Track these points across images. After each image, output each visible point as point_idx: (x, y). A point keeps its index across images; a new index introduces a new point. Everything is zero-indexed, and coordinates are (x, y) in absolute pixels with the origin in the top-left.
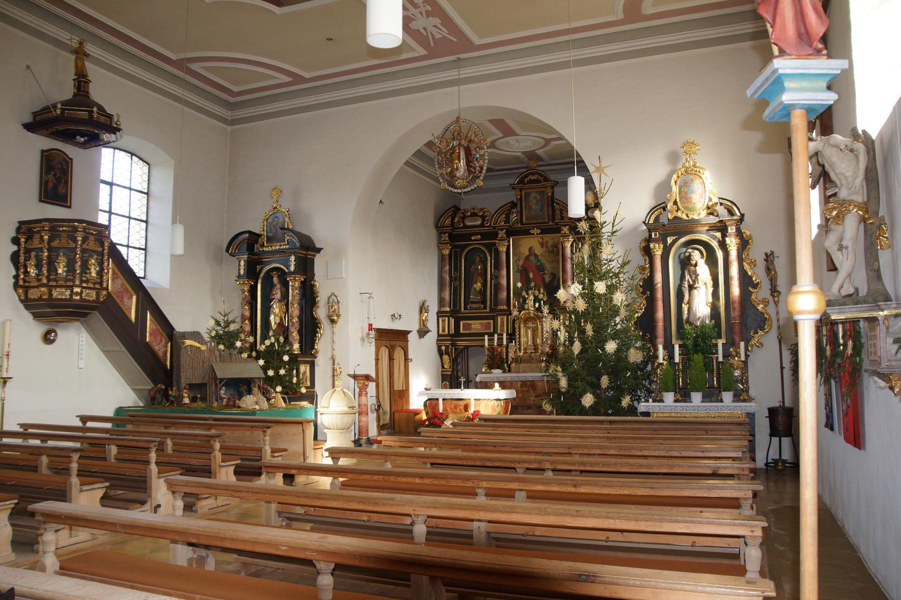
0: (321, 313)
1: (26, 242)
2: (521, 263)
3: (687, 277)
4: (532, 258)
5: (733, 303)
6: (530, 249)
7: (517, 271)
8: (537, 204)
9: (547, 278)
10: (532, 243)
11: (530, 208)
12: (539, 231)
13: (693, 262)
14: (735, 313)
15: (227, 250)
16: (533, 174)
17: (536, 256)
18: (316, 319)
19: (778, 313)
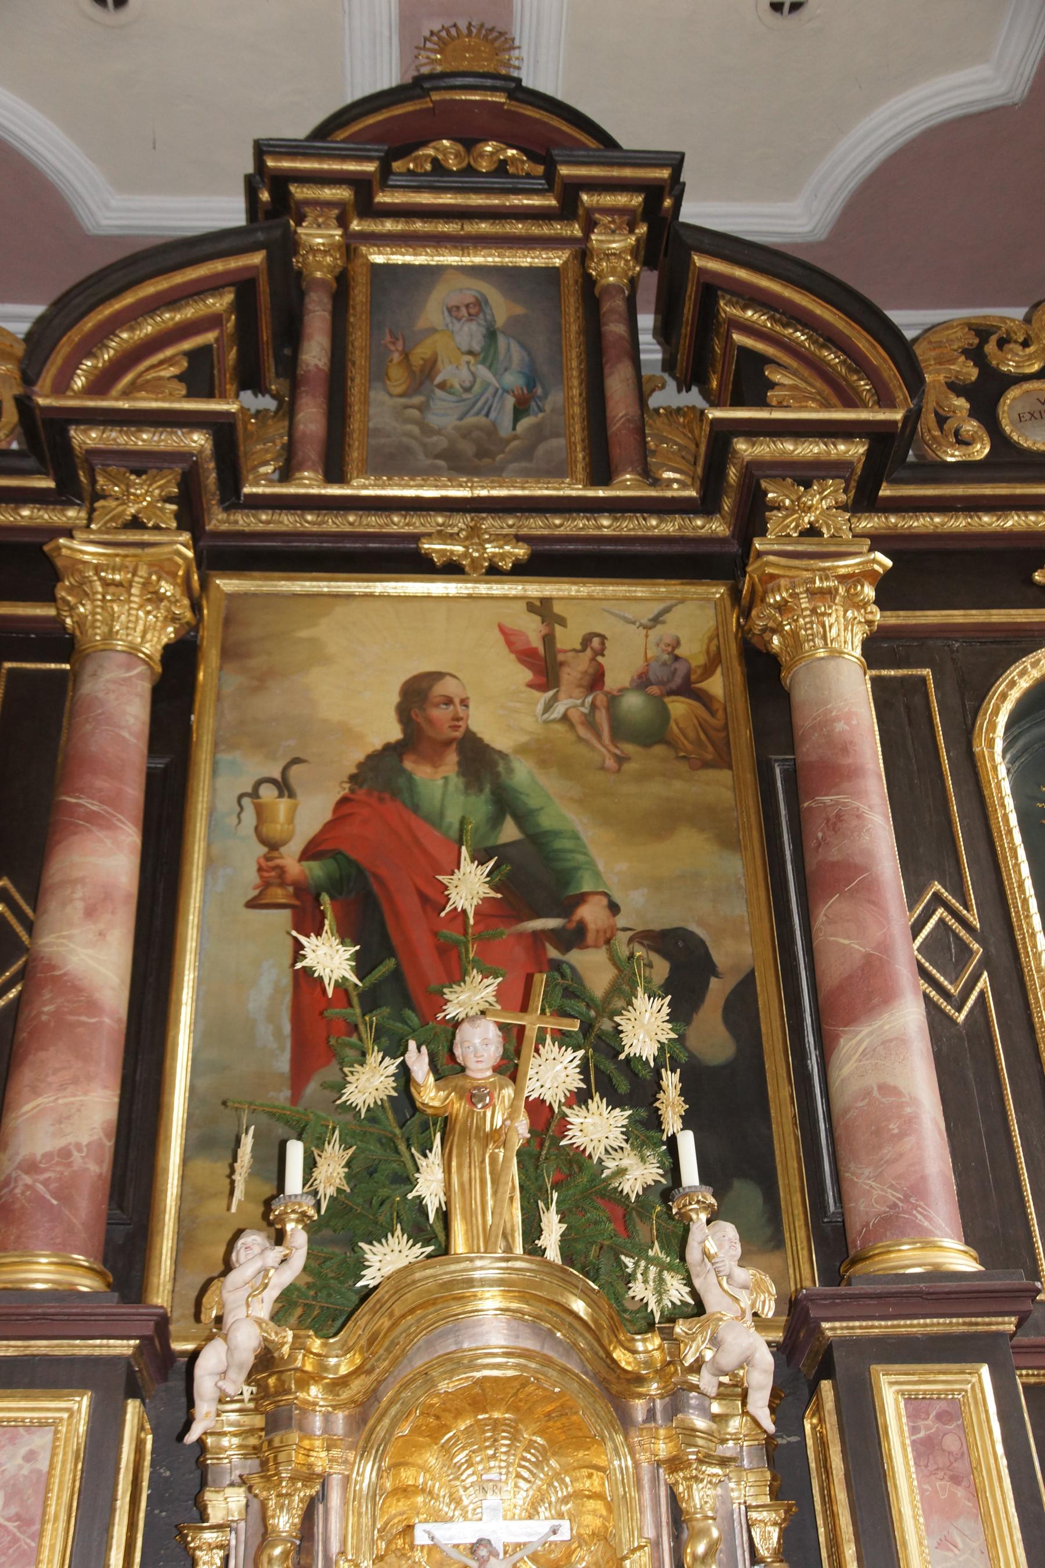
2: (310, 813)
4: (437, 782)
6: (416, 694)
8: (487, 352)
11: (424, 377)
17: (477, 760)
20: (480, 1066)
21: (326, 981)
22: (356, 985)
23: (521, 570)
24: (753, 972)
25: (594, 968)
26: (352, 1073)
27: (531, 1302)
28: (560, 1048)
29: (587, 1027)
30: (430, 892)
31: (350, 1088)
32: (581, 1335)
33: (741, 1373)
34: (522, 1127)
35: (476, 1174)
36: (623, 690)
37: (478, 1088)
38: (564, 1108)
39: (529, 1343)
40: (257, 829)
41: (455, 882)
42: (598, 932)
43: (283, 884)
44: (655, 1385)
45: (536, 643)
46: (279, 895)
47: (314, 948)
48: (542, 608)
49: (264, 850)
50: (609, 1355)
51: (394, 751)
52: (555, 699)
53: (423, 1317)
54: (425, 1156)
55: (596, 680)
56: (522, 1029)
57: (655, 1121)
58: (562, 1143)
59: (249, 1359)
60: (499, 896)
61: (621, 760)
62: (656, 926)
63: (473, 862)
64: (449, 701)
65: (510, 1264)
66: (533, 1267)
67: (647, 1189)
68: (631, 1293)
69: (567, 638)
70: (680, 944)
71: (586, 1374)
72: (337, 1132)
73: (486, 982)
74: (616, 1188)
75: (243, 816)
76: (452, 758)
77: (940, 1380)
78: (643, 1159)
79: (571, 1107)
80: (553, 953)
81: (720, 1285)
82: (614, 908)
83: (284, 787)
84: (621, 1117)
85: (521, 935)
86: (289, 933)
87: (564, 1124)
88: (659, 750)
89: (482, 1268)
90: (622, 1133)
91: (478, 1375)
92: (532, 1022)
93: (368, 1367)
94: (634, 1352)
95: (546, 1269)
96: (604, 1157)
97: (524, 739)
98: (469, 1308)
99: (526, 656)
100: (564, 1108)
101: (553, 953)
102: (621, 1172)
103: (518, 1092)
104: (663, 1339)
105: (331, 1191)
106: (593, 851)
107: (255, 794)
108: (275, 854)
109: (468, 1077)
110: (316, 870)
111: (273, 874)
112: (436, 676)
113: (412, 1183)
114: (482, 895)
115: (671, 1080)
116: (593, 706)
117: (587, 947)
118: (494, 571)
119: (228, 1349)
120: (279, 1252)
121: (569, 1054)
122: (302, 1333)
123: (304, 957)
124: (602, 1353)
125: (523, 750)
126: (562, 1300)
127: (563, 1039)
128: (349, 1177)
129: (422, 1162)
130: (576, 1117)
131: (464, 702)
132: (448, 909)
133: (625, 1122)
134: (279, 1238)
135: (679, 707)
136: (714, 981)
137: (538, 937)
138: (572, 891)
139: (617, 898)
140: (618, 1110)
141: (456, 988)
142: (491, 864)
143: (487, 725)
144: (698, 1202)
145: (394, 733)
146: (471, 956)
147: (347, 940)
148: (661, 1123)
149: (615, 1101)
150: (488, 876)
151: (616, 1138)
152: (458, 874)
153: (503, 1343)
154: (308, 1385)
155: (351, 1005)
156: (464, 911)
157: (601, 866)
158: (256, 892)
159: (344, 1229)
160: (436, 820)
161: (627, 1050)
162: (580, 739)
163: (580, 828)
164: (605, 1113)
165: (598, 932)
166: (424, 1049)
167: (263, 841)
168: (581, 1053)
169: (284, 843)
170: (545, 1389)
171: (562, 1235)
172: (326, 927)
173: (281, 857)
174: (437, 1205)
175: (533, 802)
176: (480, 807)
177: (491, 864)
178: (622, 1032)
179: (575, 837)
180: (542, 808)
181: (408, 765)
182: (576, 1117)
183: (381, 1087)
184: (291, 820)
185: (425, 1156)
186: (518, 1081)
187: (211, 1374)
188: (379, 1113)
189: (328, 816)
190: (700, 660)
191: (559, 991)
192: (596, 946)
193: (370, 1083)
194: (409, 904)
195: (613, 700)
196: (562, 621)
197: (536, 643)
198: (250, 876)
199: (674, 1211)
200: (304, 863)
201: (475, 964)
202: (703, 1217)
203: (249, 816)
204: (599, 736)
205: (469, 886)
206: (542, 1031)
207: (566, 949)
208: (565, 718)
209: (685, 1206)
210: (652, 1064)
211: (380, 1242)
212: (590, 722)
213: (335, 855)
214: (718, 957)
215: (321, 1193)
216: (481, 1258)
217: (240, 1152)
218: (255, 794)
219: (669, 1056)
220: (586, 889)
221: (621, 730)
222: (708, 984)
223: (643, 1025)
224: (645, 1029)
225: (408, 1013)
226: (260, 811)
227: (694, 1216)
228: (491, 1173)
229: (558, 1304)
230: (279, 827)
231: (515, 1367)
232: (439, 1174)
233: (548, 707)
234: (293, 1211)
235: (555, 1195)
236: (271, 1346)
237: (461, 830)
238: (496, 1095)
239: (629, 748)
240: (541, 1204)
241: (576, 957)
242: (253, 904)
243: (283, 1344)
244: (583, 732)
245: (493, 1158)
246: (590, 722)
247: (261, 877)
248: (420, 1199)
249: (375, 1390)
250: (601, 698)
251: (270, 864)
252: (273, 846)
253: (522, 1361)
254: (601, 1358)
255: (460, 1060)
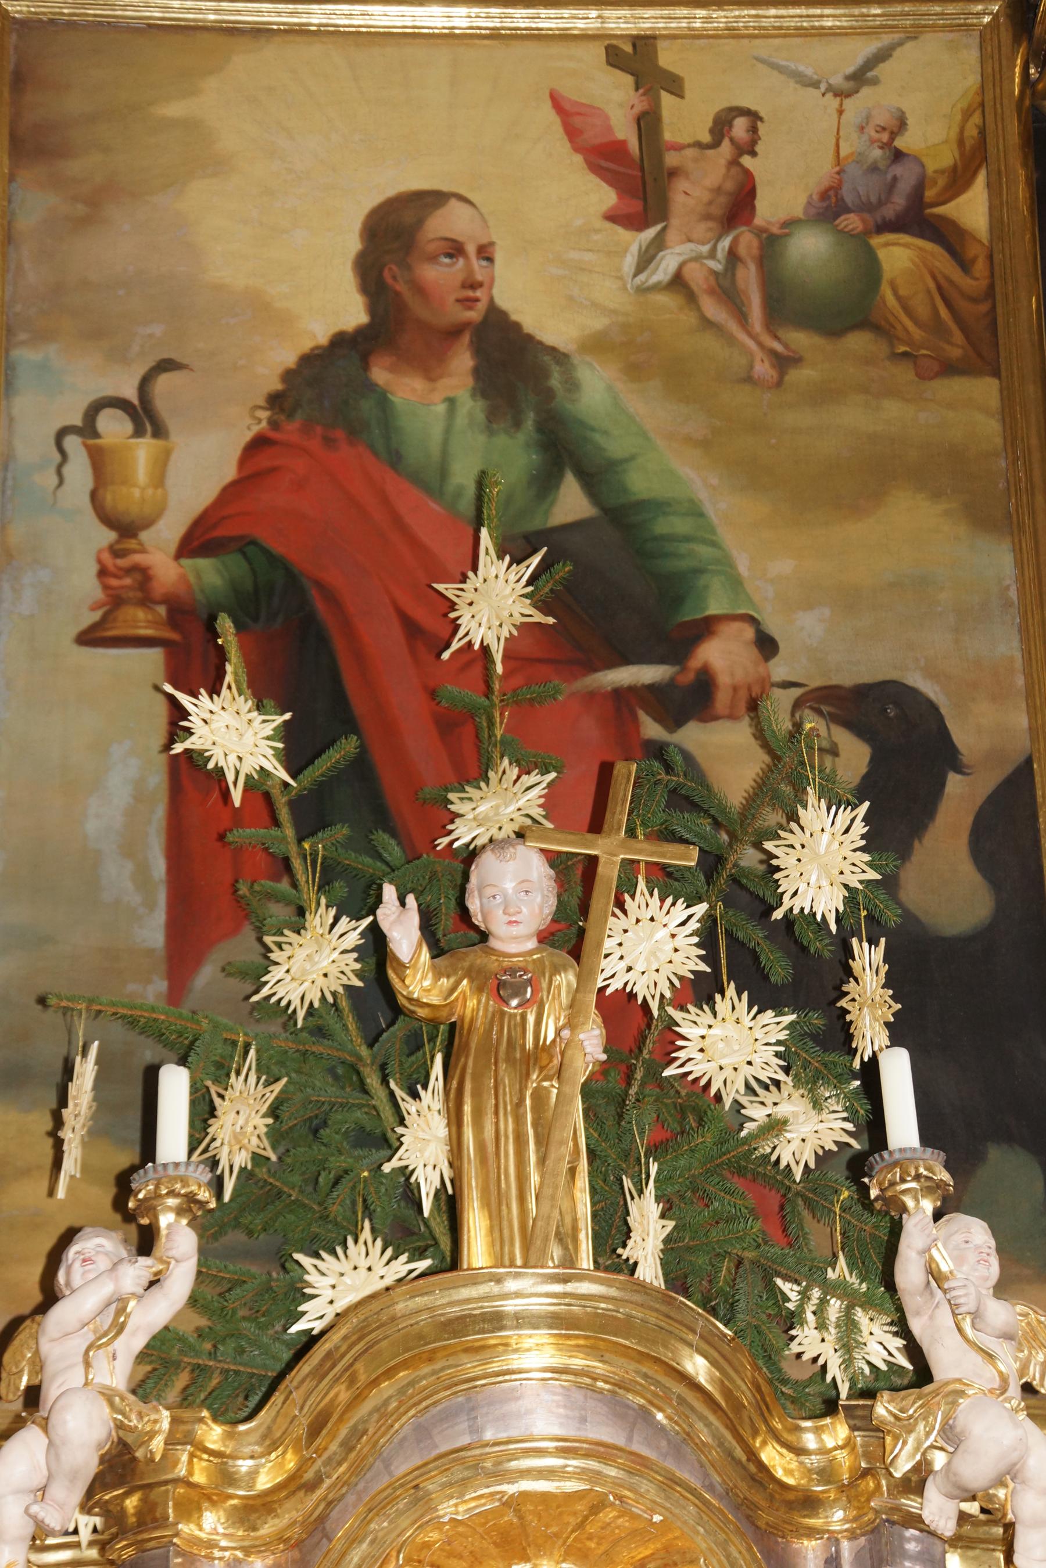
2: (195, 467)
4: (434, 407)
6: (393, 236)
17: (510, 364)
20: (515, 930)
21: (230, 777)
22: (286, 785)
24: (1029, 762)
25: (726, 754)
26: (279, 946)
27: (607, 1356)
28: (662, 901)
29: (712, 862)
30: (420, 614)
31: (276, 973)
32: (702, 1418)
33: (1001, 1493)
34: (591, 1043)
35: (509, 1126)
36: (790, 224)
37: (512, 971)
38: (670, 1010)
39: (605, 1431)
40: (94, 495)
41: (469, 596)
42: (735, 689)
43: (146, 600)
44: (839, 1514)
45: (624, 131)
46: (140, 620)
47: (207, 716)
48: (635, 57)
49: (110, 536)
50: (753, 1456)
51: (351, 348)
52: (659, 244)
53: (411, 1384)
54: (415, 1096)
55: (738, 204)
56: (593, 860)
57: (840, 1034)
58: (666, 1073)
59: (90, 1466)
60: (551, 620)
61: (784, 362)
62: (847, 679)
63: (500, 557)
64: (455, 249)
65: (570, 1287)
66: (613, 1292)
67: (824, 1158)
68: (795, 1348)
69: (685, 120)
70: (891, 712)
71: (711, 1488)
72: (252, 1053)
73: (527, 780)
74: (766, 1157)
75: (66, 470)
76: (463, 361)
78: (817, 1105)
79: (683, 1008)
80: (652, 729)
81: (960, 1330)
82: (766, 645)
83: (144, 416)
84: (776, 1025)
85: (592, 697)
86: (158, 689)
87: (671, 1039)
88: (858, 341)
89: (518, 1295)
90: (777, 1055)
91: (511, 1489)
92: (610, 851)
93: (309, 1475)
94: (800, 1451)
95: (637, 1298)
96: (744, 1100)
97: (597, 323)
98: (495, 1367)
99: (604, 158)
100: (670, 1010)
101: (652, 729)
102: (776, 1126)
103: (584, 979)
104: (853, 1428)
105: (242, 1159)
106: (727, 537)
107: (88, 429)
108: (132, 544)
109: (493, 951)
110: (208, 574)
111: (128, 581)
112: (431, 200)
113: (390, 1145)
114: (519, 620)
115: (869, 960)
116: (733, 256)
117: (716, 718)
119: (51, 1444)
120: (144, 1266)
121: (680, 911)
122: (186, 1414)
123: (189, 732)
124: (739, 1453)
125: (597, 345)
126: (666, 1356)
127: (668, 882)
128: (275, 1136)
129: (409, 1106)
130: (692, 1025)
131: (485, 253)
132: (455, 645)
133: (783, 1036)
134: (146, 1242)
135: (899, 256)
136: (954, 782)
137: (624, 698)
138: (689, 614)
139: (773, 627)
140: (770, 1013)
141: (471, 791)
142: (535, 560)
143: (530, 296)
144: (918, 1177)
145: (352, 312)
146: (499, 732)
147: (268, 703)
148: (850, 1037)
149: (765, 997)
150: (529, 583)
151: (766, 1064)
152: (474, 581)
153: (557, 1431)
154: (200, 1510)
155: (276, 823)
156: (485, 649)
157: (743, 567)
158: (97, 616)
159: (264, 1229)
160: (432, 481)
161: (787, 902)
162: (707, 324)
163: (703, 495)
164: (746, 1021)
165: (735, 689)
166: (411, 900)
167: (108, 520)
168: (701, 909)
169: (148, 523)
170: (634, 1517)
171: (667, 1241)
172: (229, 678)
173: (143, 551)
174: (437, 1183)
175: (616, 447)
176: (514, 456)
177: (535, 560)
178: (778, 869)
179: (696, 512)
180: (632, 458)
181: (379, 375)
182: (692, 1025)
183: (333, 971)
184: (159, 478)
185: (415, 1096)
186: (584, 958)
187: (18, 1492)
188: (331, 1021)
189: (230, 473)
190: (946, 158)
191: (661, 796)
192: (732, 717)
193: (313, 964)
194: (383, 638)
195: (771, 244)
196: (675, 85)
197: (624, 131)
198: (83, 586)
199: (874, 1193)
200: (186, 562)
201: (507, 748)
202: (928, 1206)
203: (79, 472)
204: (742, 317)
205: (494, 603)
206: (630, 865)
207: (675, 720)
208: (678, 282)
209: (892, 1184)
210: (833, 928)
211: (333, 1253)
212: (726, 290)
213: (244, 545)
214: (963, 736)
215: (224, 1163)
216: (517, 1275)
217: (73, 1089)
218: (88, 429)
219: (863, 913)
220: (714, 608)
221: (784, 304)
222: (943, 785)
223: (817, 855)
224: (821, 863)
225: (382, 837)
226: (98, 459)
227: (910, 1203)
228: (535, 1125)
229: (657, 1360)
230: (136, 493)
231: (582, 1474)
232: (439, 1127)
233: (646, 261)
234: (172, 1193)
235: (654, 1168)
236: (129, 1439)
237: (480, 499)
238: (544, 985)
239: (800, 339)
240: (627, 1183)
241: (693, 737)
242: (89, 638)
243: (152, 1435)
244: (712, 309)
245: (540, 1097)
246: (726, 290)
247: (106, 587)
248: (406, 1172)
249: (322, 1519)
250: (747, 241)
251: (121, 562)
252: (126, 528)
253: (593, 1464)
254: (739, 1462)
255: (478, 920)
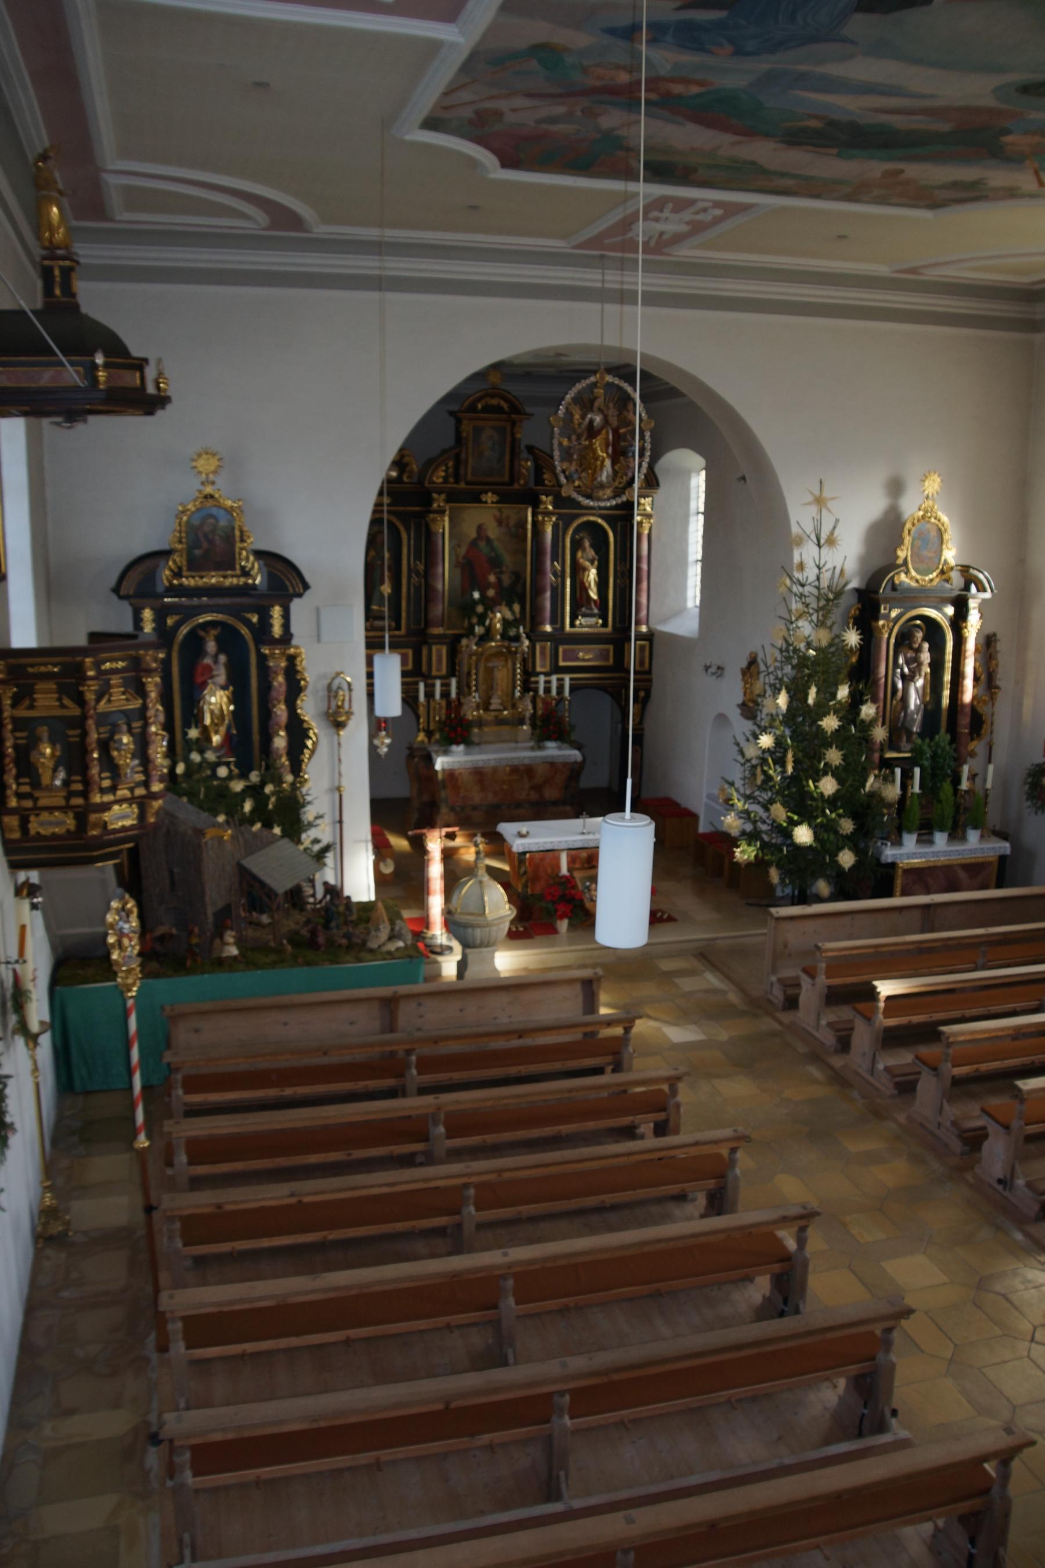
0: (309, 708)
1: (13, 706)
2: (463, 551)
3: (901, 661)
4: (482, 544)
5: (963, 706)
6: (480, 528)
7: (455, 564)
9: (506, 580)
10: (484, 517)
12: (495, 498)
13: (916, 646)
14: (964, 721)
15: (116, 590)
16: (493, 396)
17: (489, 541)
18: (304, 721)
19: (993, 715)
23: (497, 502)
55: (507, 525)
77: (543, 644)
83: (459, 546)
118: (493, 503)
